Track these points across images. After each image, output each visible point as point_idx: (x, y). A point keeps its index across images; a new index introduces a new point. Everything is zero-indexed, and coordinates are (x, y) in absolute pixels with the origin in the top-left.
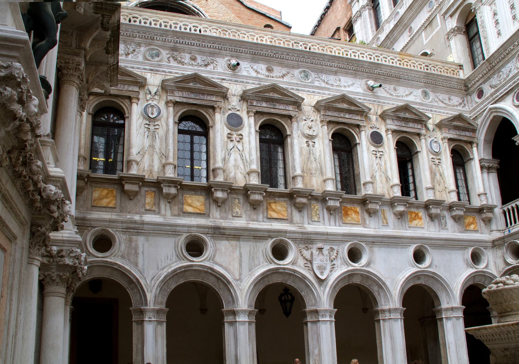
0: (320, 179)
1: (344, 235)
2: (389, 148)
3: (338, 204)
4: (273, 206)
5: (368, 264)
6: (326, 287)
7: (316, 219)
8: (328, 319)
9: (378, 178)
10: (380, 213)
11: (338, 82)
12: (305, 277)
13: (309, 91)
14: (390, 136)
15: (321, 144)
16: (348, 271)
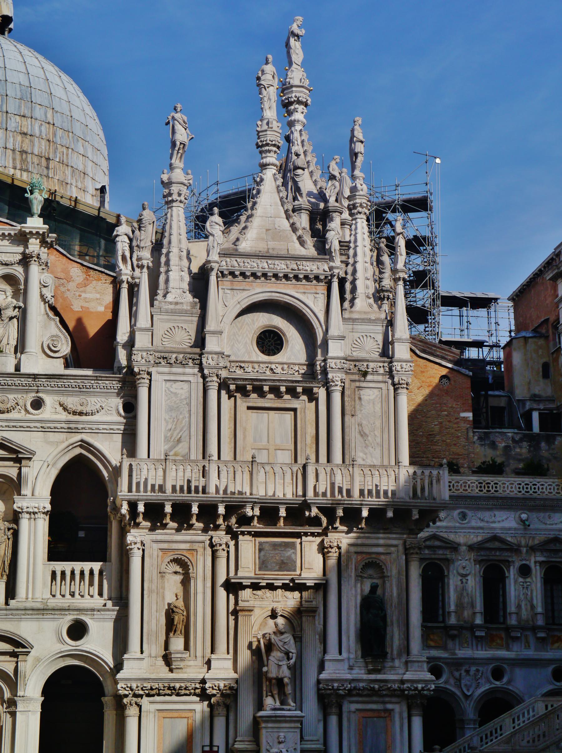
0: (470, 612)
1: (488, 659)
2: (536, 578)
3: (483, 634)
4: (432, 637)
5: (509, 682)
6: (471, 701)
7: (466, 645)
8: (472, 726)
9: (523, 607)
10: (523, 638)
11: (493, 518)
12: (455, 694)
13: (465, 532)
14: (538, 568)
15: (473, 580)
16: (490, 688)
